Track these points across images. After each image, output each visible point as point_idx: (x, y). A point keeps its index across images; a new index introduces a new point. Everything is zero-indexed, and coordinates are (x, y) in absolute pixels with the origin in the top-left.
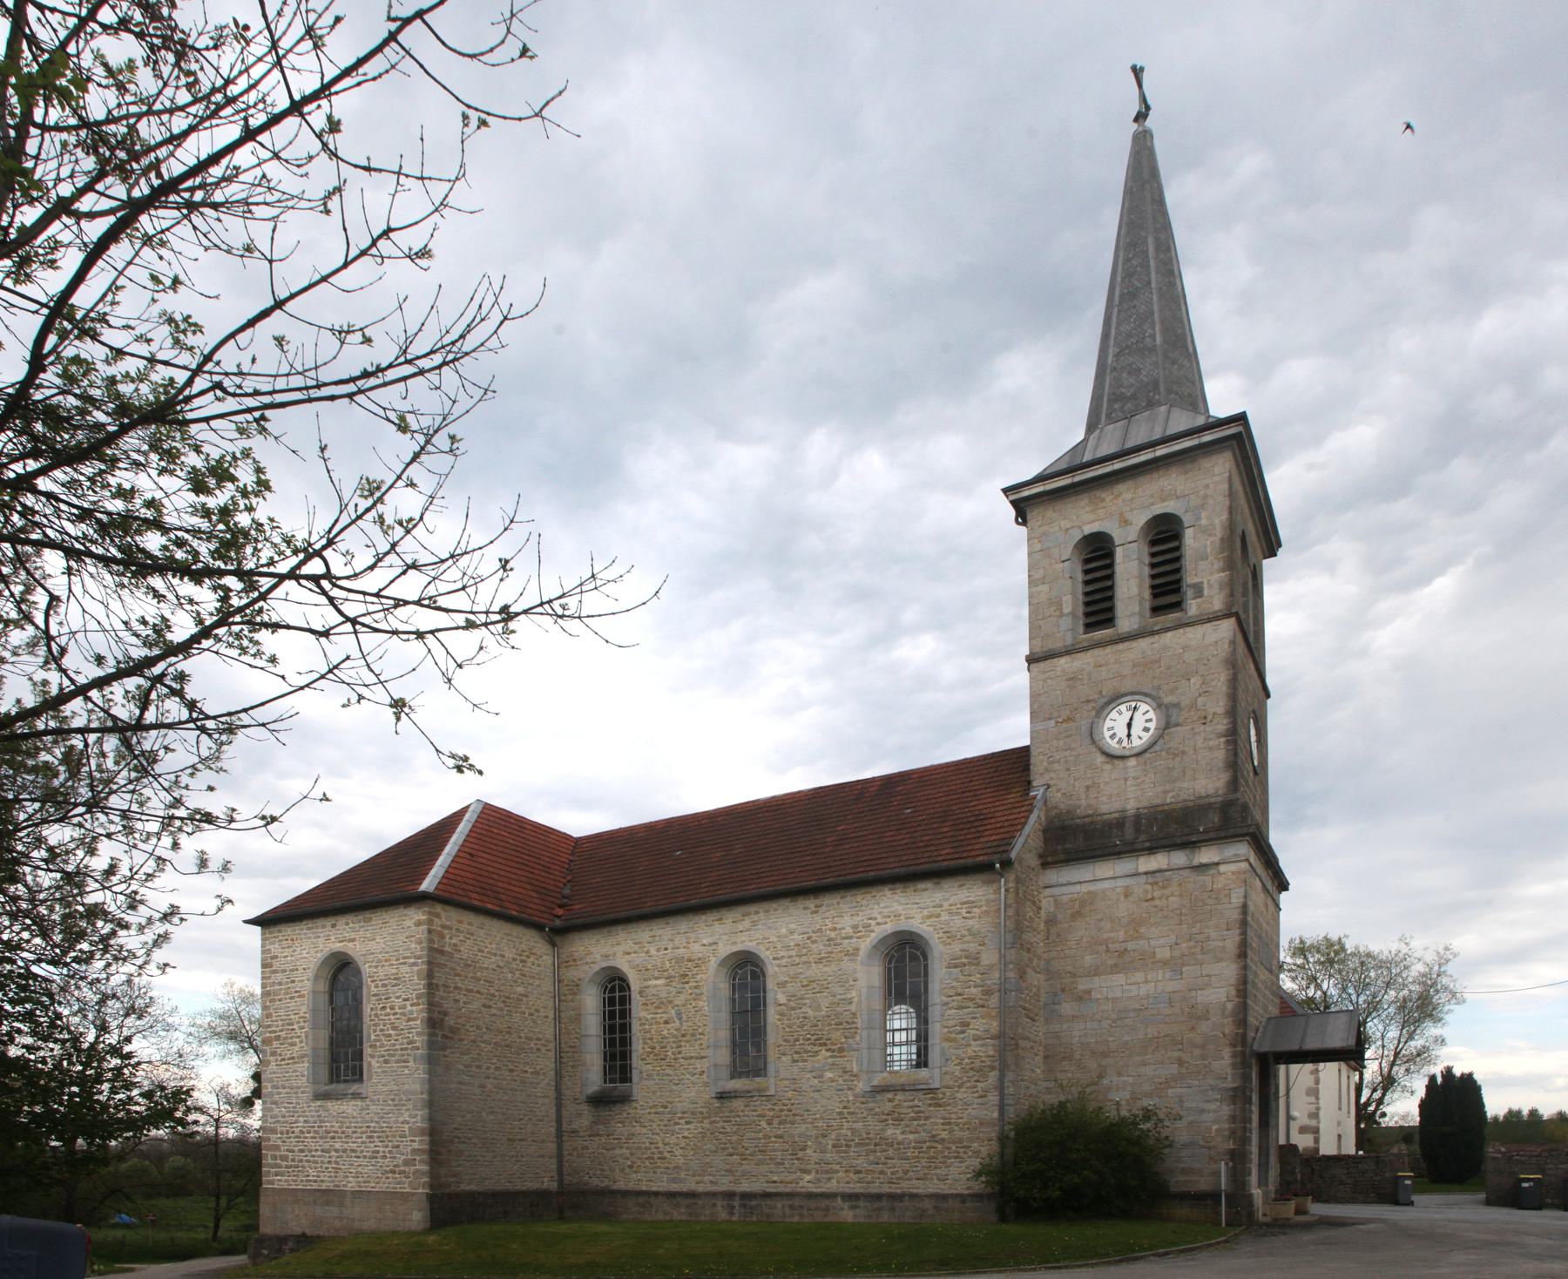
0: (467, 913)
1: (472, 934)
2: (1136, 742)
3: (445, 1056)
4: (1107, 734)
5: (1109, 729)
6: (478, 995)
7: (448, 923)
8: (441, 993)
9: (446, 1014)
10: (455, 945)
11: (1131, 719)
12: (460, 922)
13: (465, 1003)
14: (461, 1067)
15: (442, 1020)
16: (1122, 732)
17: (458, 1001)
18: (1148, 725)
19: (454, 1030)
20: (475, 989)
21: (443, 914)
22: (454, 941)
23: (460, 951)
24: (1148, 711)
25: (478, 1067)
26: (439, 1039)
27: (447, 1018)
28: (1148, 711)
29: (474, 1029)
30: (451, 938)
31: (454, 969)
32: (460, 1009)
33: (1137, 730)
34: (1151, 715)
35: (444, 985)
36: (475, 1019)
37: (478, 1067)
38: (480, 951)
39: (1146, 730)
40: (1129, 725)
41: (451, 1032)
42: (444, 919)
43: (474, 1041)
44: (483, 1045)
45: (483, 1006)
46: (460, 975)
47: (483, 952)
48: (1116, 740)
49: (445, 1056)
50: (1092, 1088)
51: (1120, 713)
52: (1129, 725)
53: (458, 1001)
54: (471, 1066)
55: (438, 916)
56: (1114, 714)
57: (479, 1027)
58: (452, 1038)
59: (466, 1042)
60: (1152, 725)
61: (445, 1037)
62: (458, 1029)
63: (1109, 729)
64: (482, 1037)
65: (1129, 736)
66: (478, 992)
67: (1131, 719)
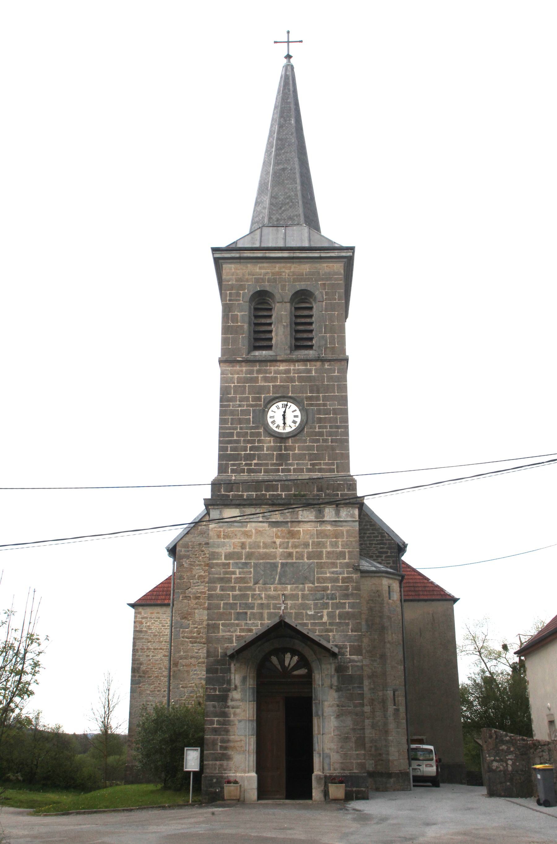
0: (156, 608)
1: (159, 618)
2: (288, 430)
3: (140, 687)
4: (270, 420)
5: (271, 417)
6: (161, 651)
7: (145, 615)
8: (140, 653)
9: (141, 664)
10: (149, 626)
11: (285, 412)
12: (152, 613)
13: (153, 656)
14: (148, 692)
15: (139, 668)
16: (280, 422)
17: (149, 656)
18: (296, 419)
19: (145, 672)
20: (159, 648)
21: (143, 612)
22: (148, 624)
23: (151, 629)
24: (295, 411)
25: (158, 691)
26: (137, 678)
27: (142, 666)
28: (295, 411)
29: (157, 670)
30: (146, 623)
31: (148, 639)
32: (150, 660)
33: (289, 421)
34: (298, 413)
35: (141, 649)
36: (158, 664)
37: (158, 691)
38: (163, 626)
39: (294, 422)
40: (284, 416)
41: (144, 673)
42: (143, 614)
43: (156, 677)
44: (162, 678)
45: (163, 656)
46: (150, 642)
47: (165, 626)
48: (276, 425)
49: (140, 687)
50: (475, 653)
51: (278, 408)
52: (284, 416)
53: (149, 656)
54: (154, 691)
55: (140, 613)
56: (274, 408)
57: (160, 668)
58: (144, 677)
59: (152, 678)
60: (298, 420)
61: (140, 676)
62: (148, 671)
63: (271, 417)
64: (162, 674)
65: (284, 423)
66: (161, 649)
67: (285, 412)
